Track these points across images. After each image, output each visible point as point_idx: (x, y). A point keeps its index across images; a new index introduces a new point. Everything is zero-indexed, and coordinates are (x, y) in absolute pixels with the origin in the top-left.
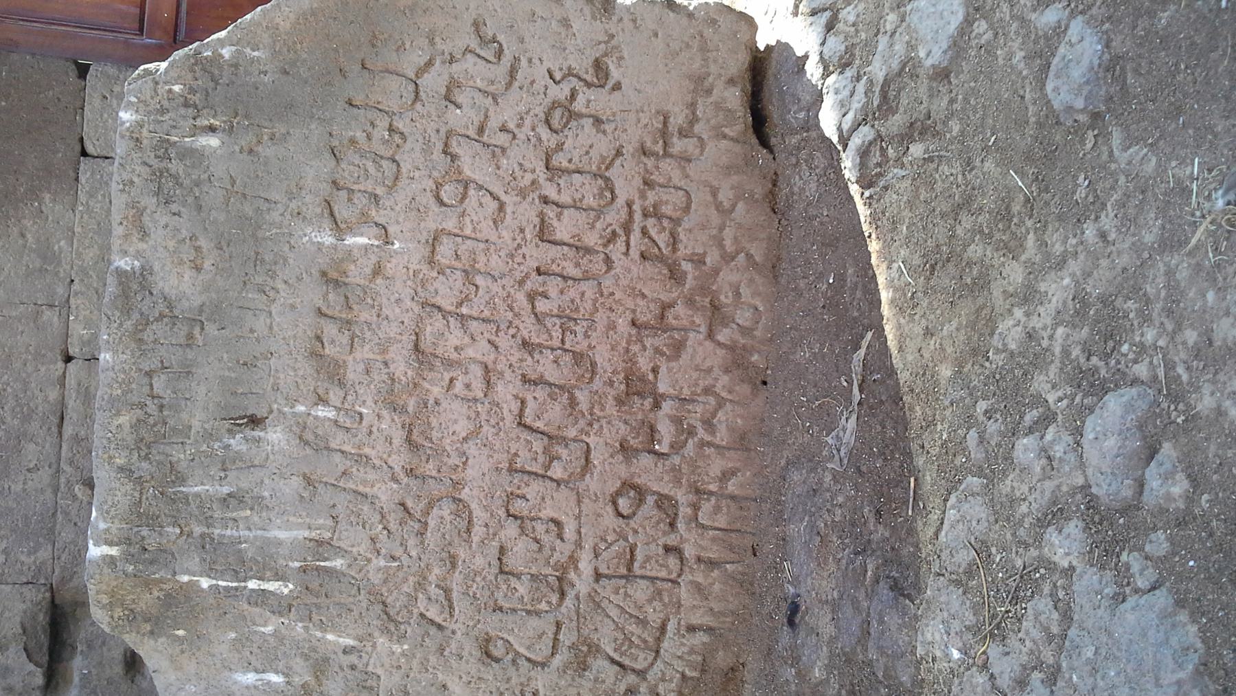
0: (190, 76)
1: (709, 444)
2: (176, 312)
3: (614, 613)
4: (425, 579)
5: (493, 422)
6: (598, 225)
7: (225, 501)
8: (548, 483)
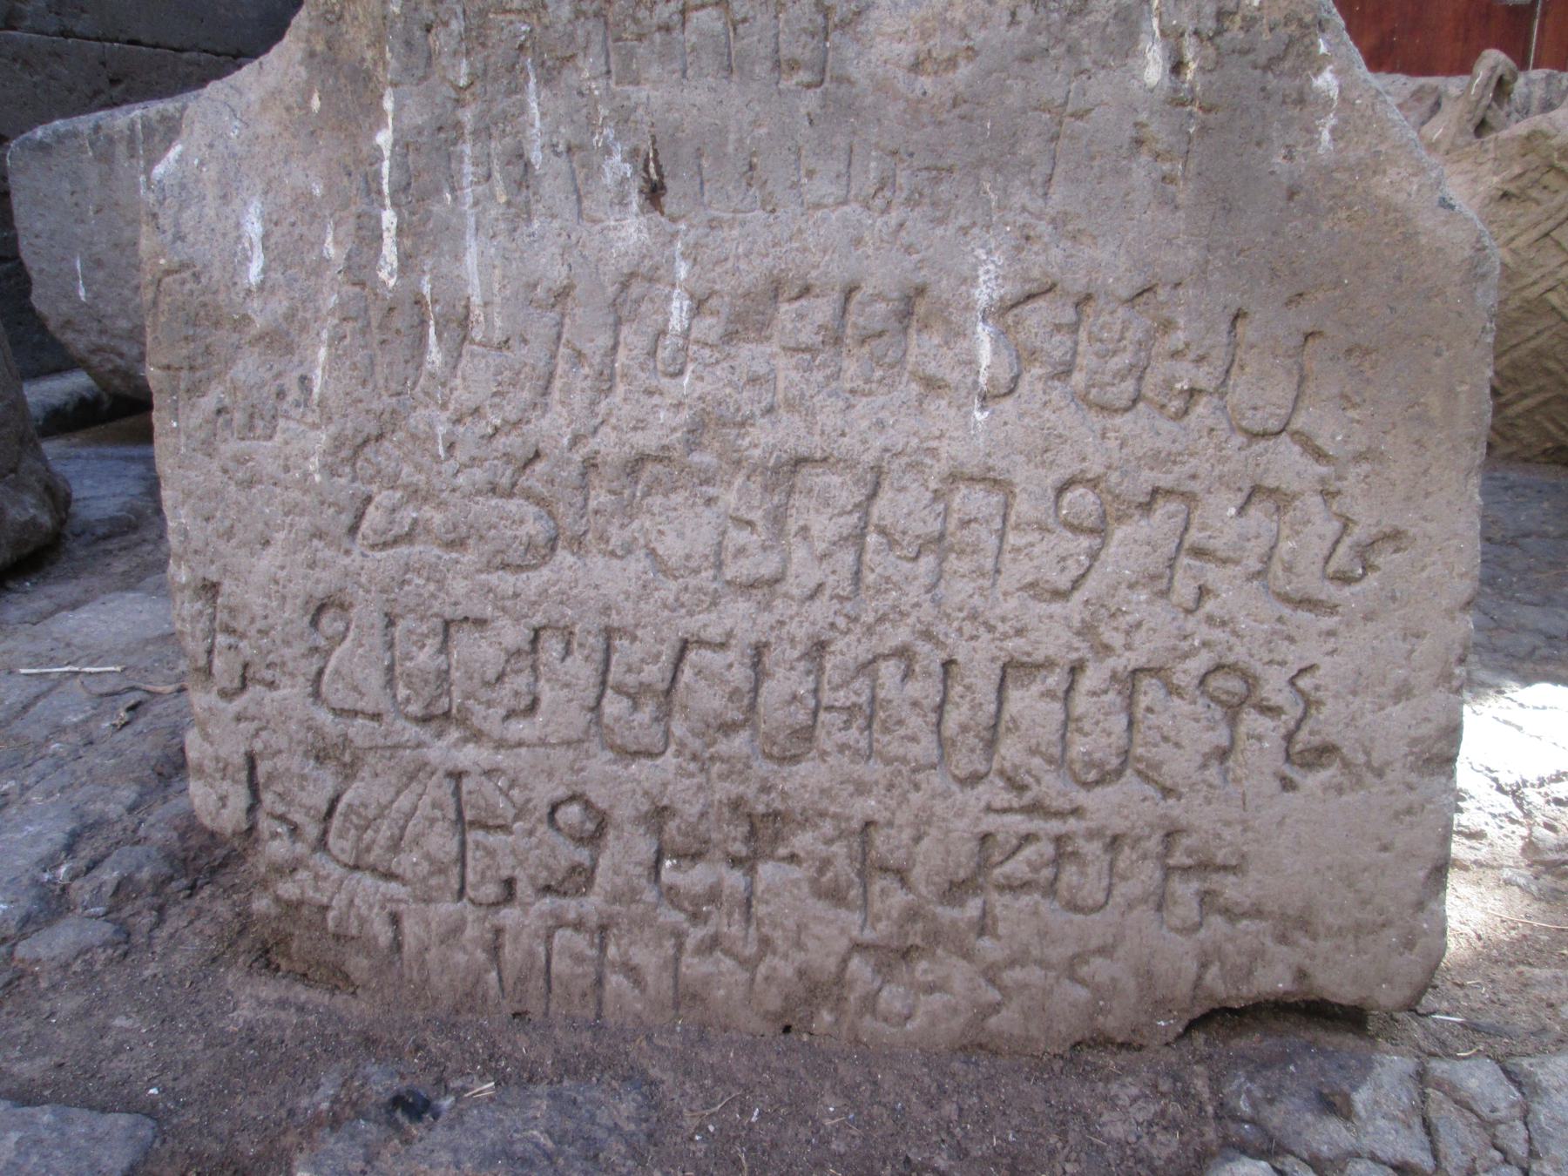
0: (1277, 16)
1: (680, 947)
2: (835, 37)
3: (404, 802)
4: (425, 499)
5: (685, 597)
6: (1037, 762)
7: (518, 155)
8: (592, 694)
